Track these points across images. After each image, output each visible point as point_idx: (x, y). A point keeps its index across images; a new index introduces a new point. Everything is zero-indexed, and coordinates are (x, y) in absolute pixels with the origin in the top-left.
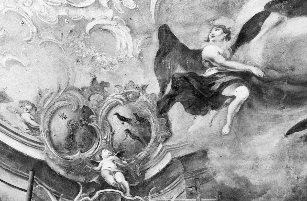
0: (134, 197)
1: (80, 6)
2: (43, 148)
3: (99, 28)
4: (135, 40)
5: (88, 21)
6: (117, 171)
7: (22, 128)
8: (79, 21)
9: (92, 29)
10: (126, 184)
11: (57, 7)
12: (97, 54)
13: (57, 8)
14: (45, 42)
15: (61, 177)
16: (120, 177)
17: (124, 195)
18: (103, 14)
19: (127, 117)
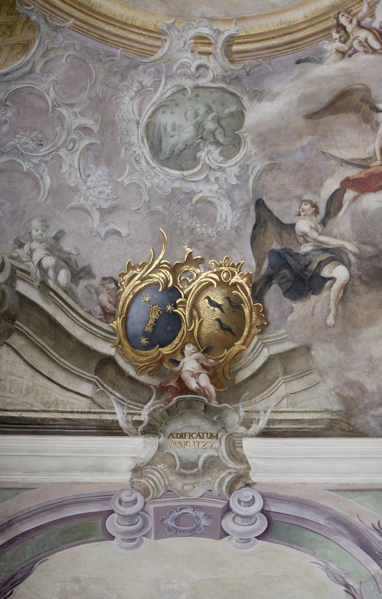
0: (220, 404)
1: (192, 180)
2: (114, 340)
3: (203, 200)
4: (234, 212)
5: (195, 193)
6: (201, 373)
7: (96, 312)
8: (189, 193)
9: (198, 200)
10: (212, 389)
11: (174, 180)
12: (198, 225)
13: (173, 181)
14: (153, 211)
15: (131, 379)
16: (204, 380)
17: (209, 401)
18: (209, 187)
19: (220, 303)
